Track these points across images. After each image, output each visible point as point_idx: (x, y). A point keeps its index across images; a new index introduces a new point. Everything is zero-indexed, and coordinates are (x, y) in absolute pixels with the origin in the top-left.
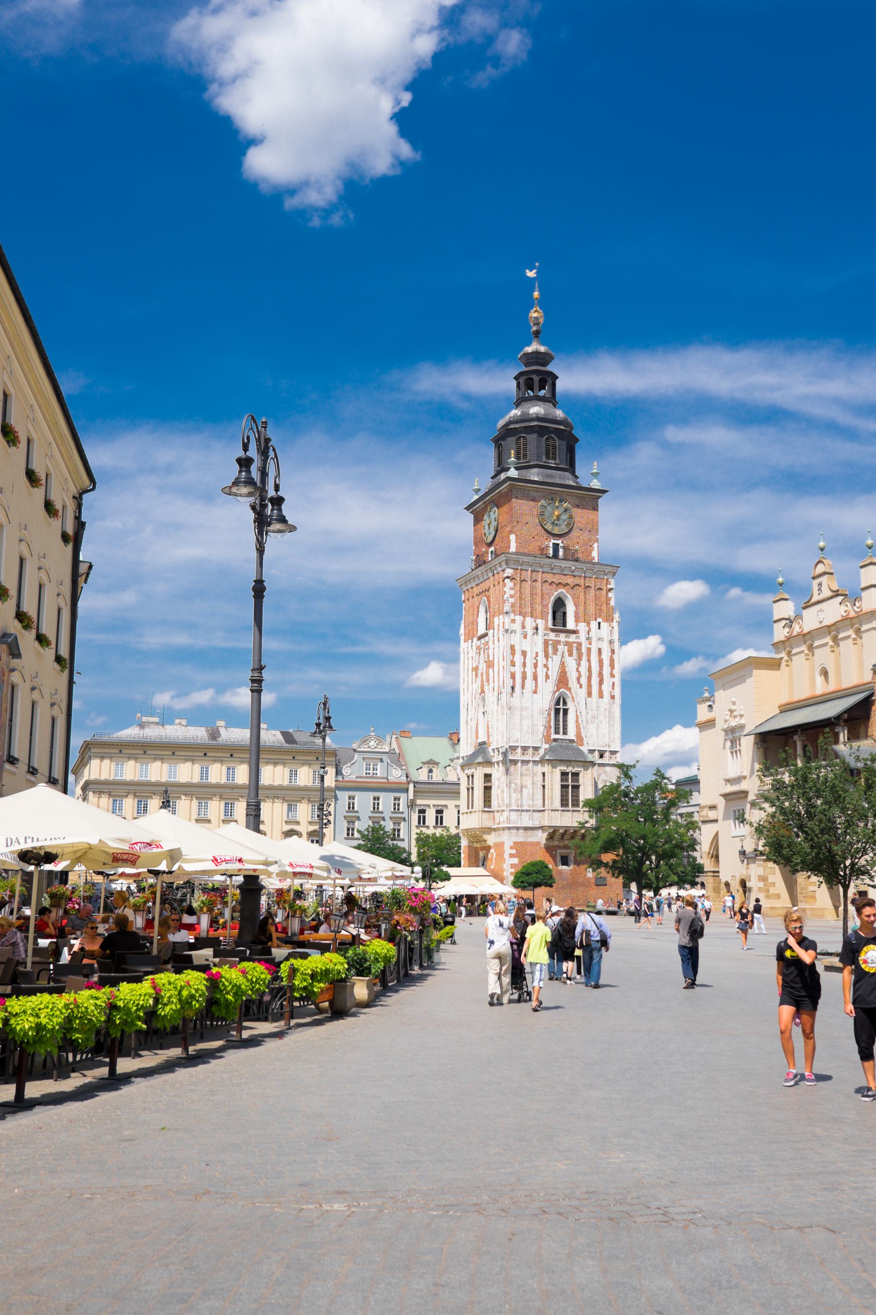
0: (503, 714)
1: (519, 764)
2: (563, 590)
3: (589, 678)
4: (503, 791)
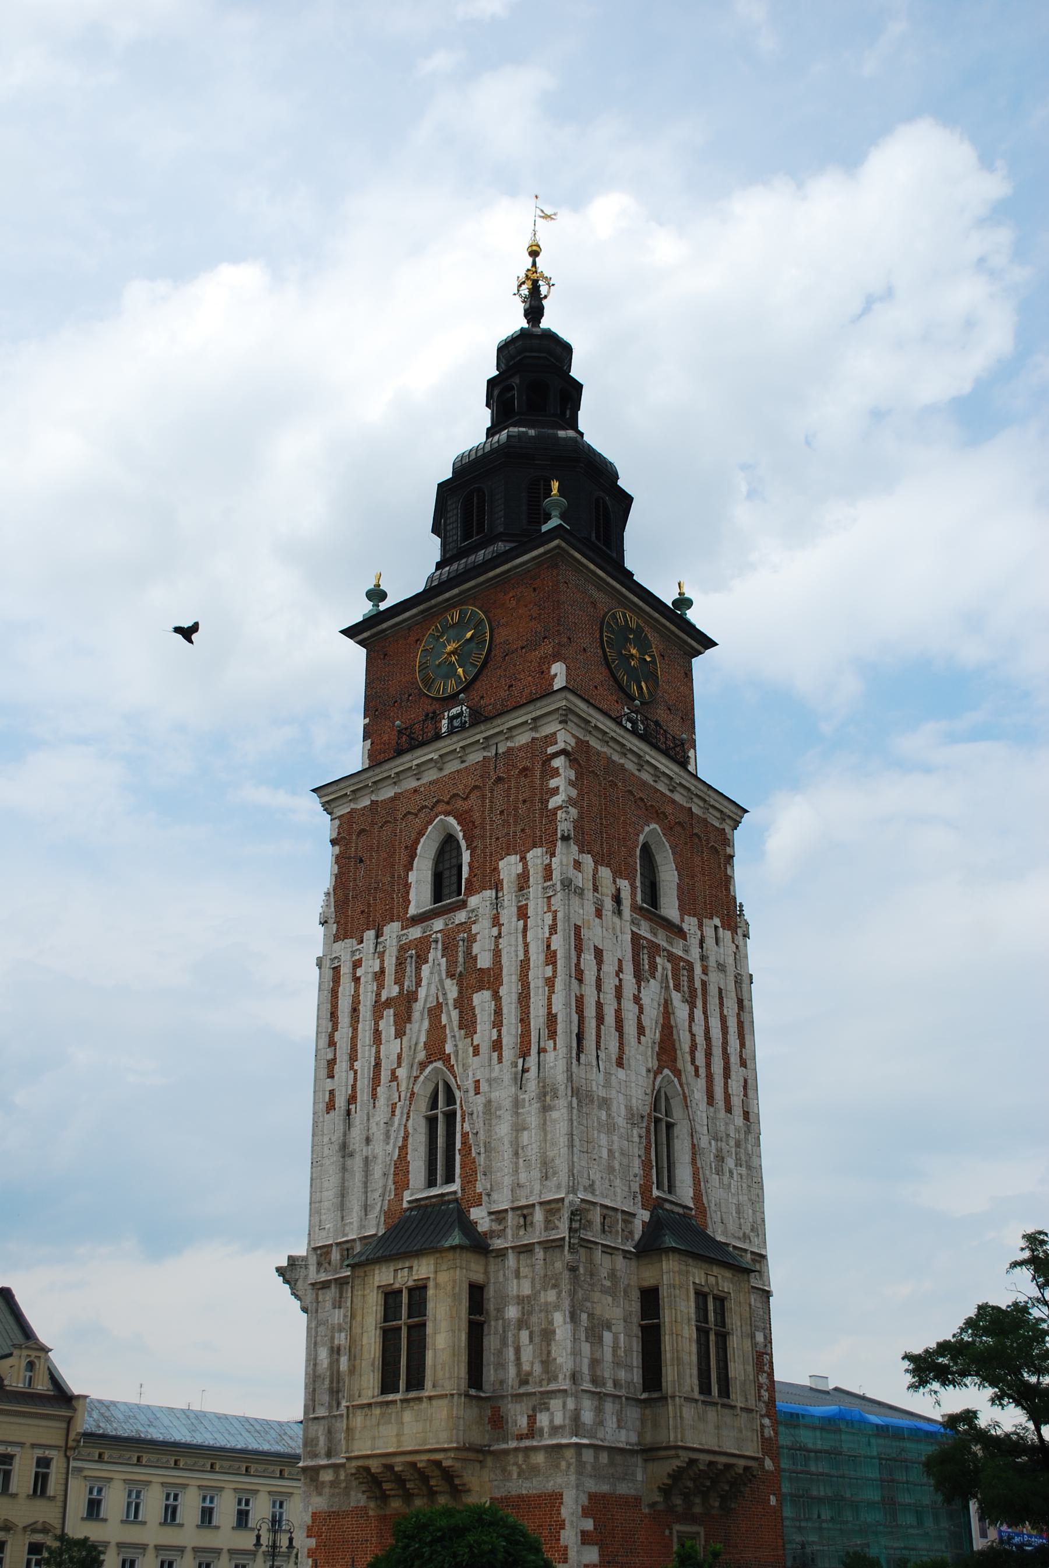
0: (545, 1109)
1: (598, 1253)
2: (657, 826)
3: (708, 1054)
4: (548, 1335)
